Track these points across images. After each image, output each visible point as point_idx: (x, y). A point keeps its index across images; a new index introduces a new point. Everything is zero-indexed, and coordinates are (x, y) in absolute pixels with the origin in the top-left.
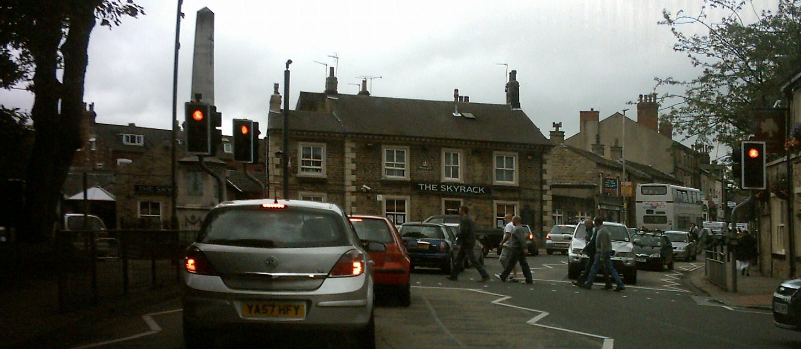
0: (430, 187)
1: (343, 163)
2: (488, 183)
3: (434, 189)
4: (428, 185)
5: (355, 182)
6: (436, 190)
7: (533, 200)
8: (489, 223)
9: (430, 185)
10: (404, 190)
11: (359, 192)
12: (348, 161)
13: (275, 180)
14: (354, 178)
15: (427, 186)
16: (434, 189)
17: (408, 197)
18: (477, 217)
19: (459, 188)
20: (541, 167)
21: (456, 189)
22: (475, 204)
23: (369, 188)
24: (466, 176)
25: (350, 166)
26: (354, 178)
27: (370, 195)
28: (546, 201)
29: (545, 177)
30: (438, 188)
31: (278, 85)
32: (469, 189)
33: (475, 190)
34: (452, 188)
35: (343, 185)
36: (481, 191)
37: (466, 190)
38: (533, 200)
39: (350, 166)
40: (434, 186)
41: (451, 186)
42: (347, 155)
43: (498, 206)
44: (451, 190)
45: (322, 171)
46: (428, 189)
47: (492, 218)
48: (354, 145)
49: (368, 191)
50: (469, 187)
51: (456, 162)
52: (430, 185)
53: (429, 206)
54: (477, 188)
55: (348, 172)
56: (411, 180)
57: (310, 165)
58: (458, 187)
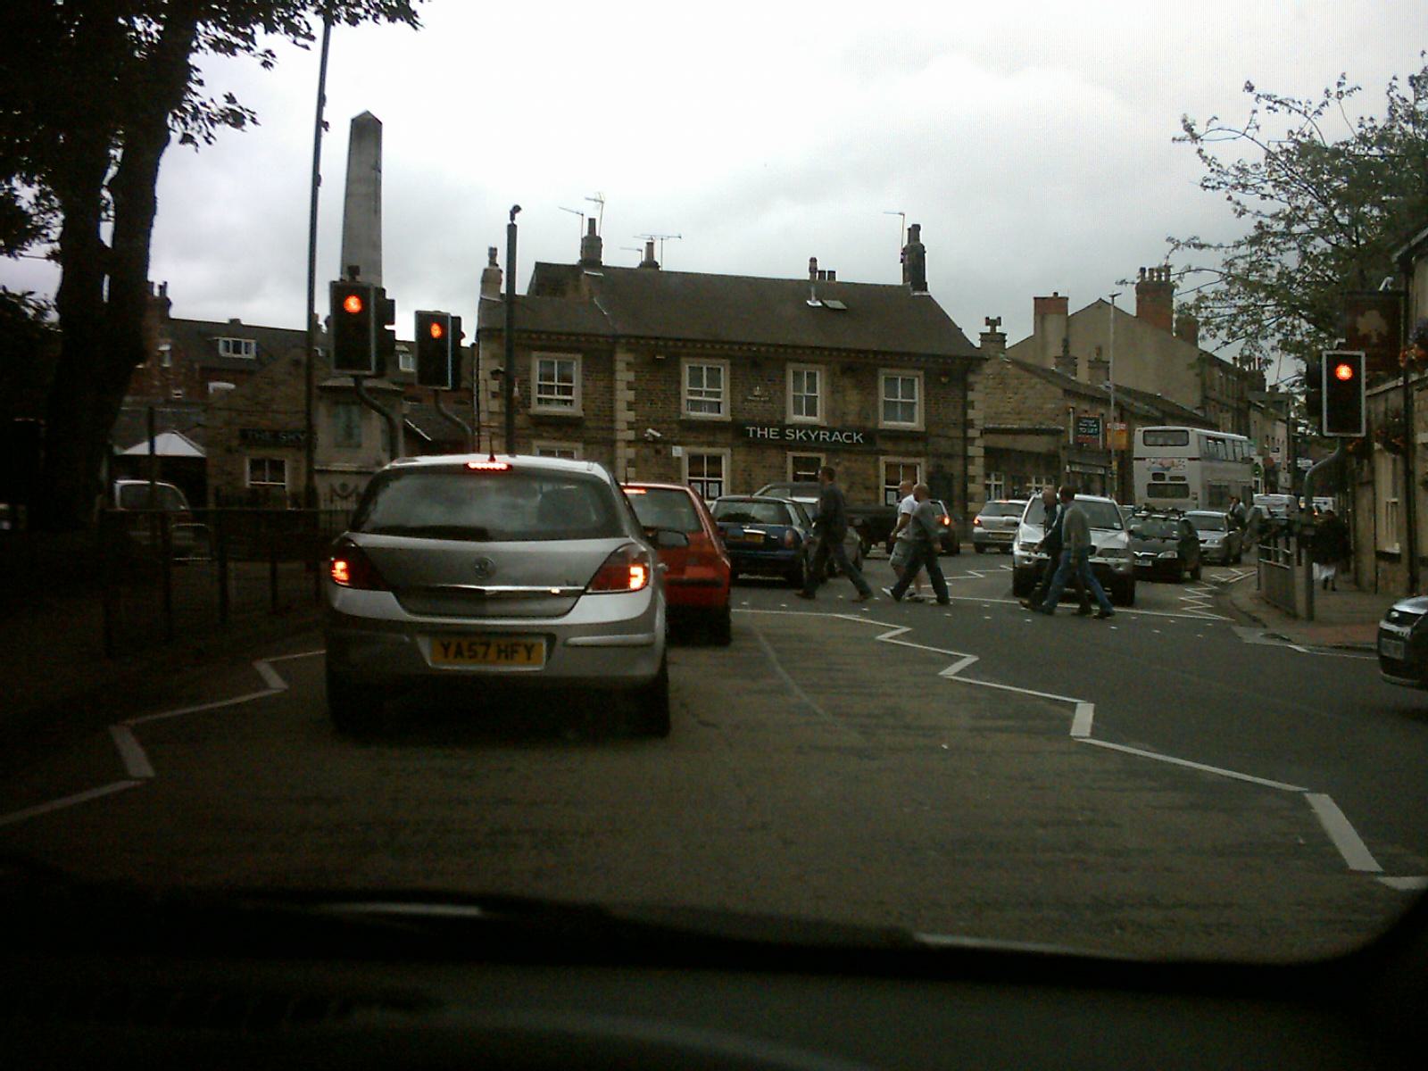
0: (766, 433)
1: (611, 389)
2: (870, 425)
4: (762, 429)
5: (633, 423)
6: (777, 437)
7: (950, 456)
8: (872, 497)
10: (720, 437)
11: (641, 441)
12: (620, 385)
13: (490, 420)
14: (631, 416)
15: (761, 430)
17: (728, 451)
19: (818, 434)
20: (965, 396)
21: (813, 437)
22: (847, 464)
23: (659, 435)
24: (831, 413)
25: (624, 396)
26: (631, 416)
27: (659, 446)
28: (973, 457)
29: (971, 414)
30: (782, 434)
31: (496, 249)
32: (837, 436)
33: (847, 437)
35: (612, 430)
36: (857, 440)
37: (830, 438)
38: (950, 456)
39: (624, 396)
41: (804, 432)
42: (619, 376)
43: (889, 466)
44: (805, 438)
45: (575, 404)
46: (762, 435)
47: (878, 488)
48: (630, 358)
49: (656, 441)
50: (837, 433)
51: (812, 388)
53: (764, 467)
55: (621, 405)
56: (733, 419)
57: (553, 393)
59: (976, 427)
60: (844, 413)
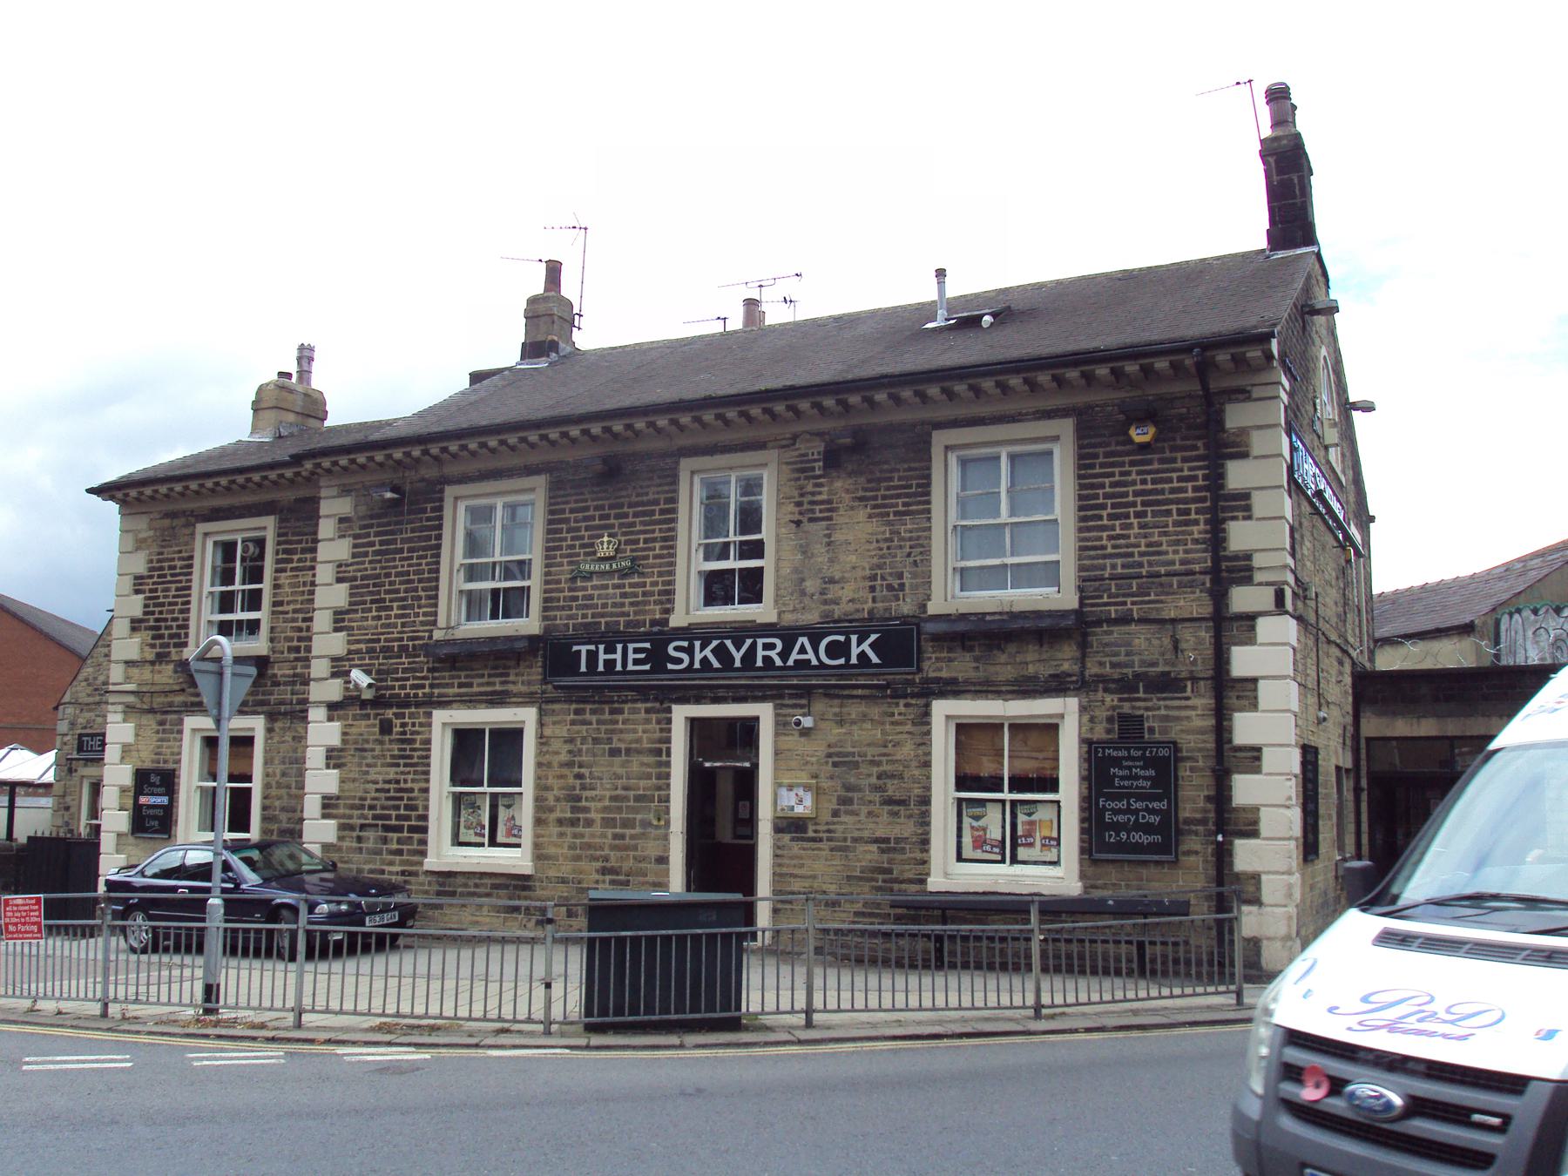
2: (906, 607)
3: (636, 662)
4: (610, 649)
6: (647, 667)
7: (1167, 684)
9: (619, 647)
13: (128, 679)
16: (636, 662)
18: (844, 801)
19: (753, 646)
20: (1216, 478)
21: (738, 656)
25: (331, 595)
27: (389, 713)
28: (1254, 680)
29: (1240, 535)
30: (657, 657)
32: (803, 650)
33: (835, 650)
34: (721, 652)
36: (862, 655)
38: (1167, 684)
39: (331, 595)
40: (636, 651)
41: (715, 643)
43: (965, 731)
44: (716, 664)
47: (925, 801)
48: (344, 506)
50: (804, 640)
52: (619, 647)
53: (614, 752)
54: (842, 638)
56: (547, 629)
58: (749, 642)
59: (1259, 577)
60: (832, 581)
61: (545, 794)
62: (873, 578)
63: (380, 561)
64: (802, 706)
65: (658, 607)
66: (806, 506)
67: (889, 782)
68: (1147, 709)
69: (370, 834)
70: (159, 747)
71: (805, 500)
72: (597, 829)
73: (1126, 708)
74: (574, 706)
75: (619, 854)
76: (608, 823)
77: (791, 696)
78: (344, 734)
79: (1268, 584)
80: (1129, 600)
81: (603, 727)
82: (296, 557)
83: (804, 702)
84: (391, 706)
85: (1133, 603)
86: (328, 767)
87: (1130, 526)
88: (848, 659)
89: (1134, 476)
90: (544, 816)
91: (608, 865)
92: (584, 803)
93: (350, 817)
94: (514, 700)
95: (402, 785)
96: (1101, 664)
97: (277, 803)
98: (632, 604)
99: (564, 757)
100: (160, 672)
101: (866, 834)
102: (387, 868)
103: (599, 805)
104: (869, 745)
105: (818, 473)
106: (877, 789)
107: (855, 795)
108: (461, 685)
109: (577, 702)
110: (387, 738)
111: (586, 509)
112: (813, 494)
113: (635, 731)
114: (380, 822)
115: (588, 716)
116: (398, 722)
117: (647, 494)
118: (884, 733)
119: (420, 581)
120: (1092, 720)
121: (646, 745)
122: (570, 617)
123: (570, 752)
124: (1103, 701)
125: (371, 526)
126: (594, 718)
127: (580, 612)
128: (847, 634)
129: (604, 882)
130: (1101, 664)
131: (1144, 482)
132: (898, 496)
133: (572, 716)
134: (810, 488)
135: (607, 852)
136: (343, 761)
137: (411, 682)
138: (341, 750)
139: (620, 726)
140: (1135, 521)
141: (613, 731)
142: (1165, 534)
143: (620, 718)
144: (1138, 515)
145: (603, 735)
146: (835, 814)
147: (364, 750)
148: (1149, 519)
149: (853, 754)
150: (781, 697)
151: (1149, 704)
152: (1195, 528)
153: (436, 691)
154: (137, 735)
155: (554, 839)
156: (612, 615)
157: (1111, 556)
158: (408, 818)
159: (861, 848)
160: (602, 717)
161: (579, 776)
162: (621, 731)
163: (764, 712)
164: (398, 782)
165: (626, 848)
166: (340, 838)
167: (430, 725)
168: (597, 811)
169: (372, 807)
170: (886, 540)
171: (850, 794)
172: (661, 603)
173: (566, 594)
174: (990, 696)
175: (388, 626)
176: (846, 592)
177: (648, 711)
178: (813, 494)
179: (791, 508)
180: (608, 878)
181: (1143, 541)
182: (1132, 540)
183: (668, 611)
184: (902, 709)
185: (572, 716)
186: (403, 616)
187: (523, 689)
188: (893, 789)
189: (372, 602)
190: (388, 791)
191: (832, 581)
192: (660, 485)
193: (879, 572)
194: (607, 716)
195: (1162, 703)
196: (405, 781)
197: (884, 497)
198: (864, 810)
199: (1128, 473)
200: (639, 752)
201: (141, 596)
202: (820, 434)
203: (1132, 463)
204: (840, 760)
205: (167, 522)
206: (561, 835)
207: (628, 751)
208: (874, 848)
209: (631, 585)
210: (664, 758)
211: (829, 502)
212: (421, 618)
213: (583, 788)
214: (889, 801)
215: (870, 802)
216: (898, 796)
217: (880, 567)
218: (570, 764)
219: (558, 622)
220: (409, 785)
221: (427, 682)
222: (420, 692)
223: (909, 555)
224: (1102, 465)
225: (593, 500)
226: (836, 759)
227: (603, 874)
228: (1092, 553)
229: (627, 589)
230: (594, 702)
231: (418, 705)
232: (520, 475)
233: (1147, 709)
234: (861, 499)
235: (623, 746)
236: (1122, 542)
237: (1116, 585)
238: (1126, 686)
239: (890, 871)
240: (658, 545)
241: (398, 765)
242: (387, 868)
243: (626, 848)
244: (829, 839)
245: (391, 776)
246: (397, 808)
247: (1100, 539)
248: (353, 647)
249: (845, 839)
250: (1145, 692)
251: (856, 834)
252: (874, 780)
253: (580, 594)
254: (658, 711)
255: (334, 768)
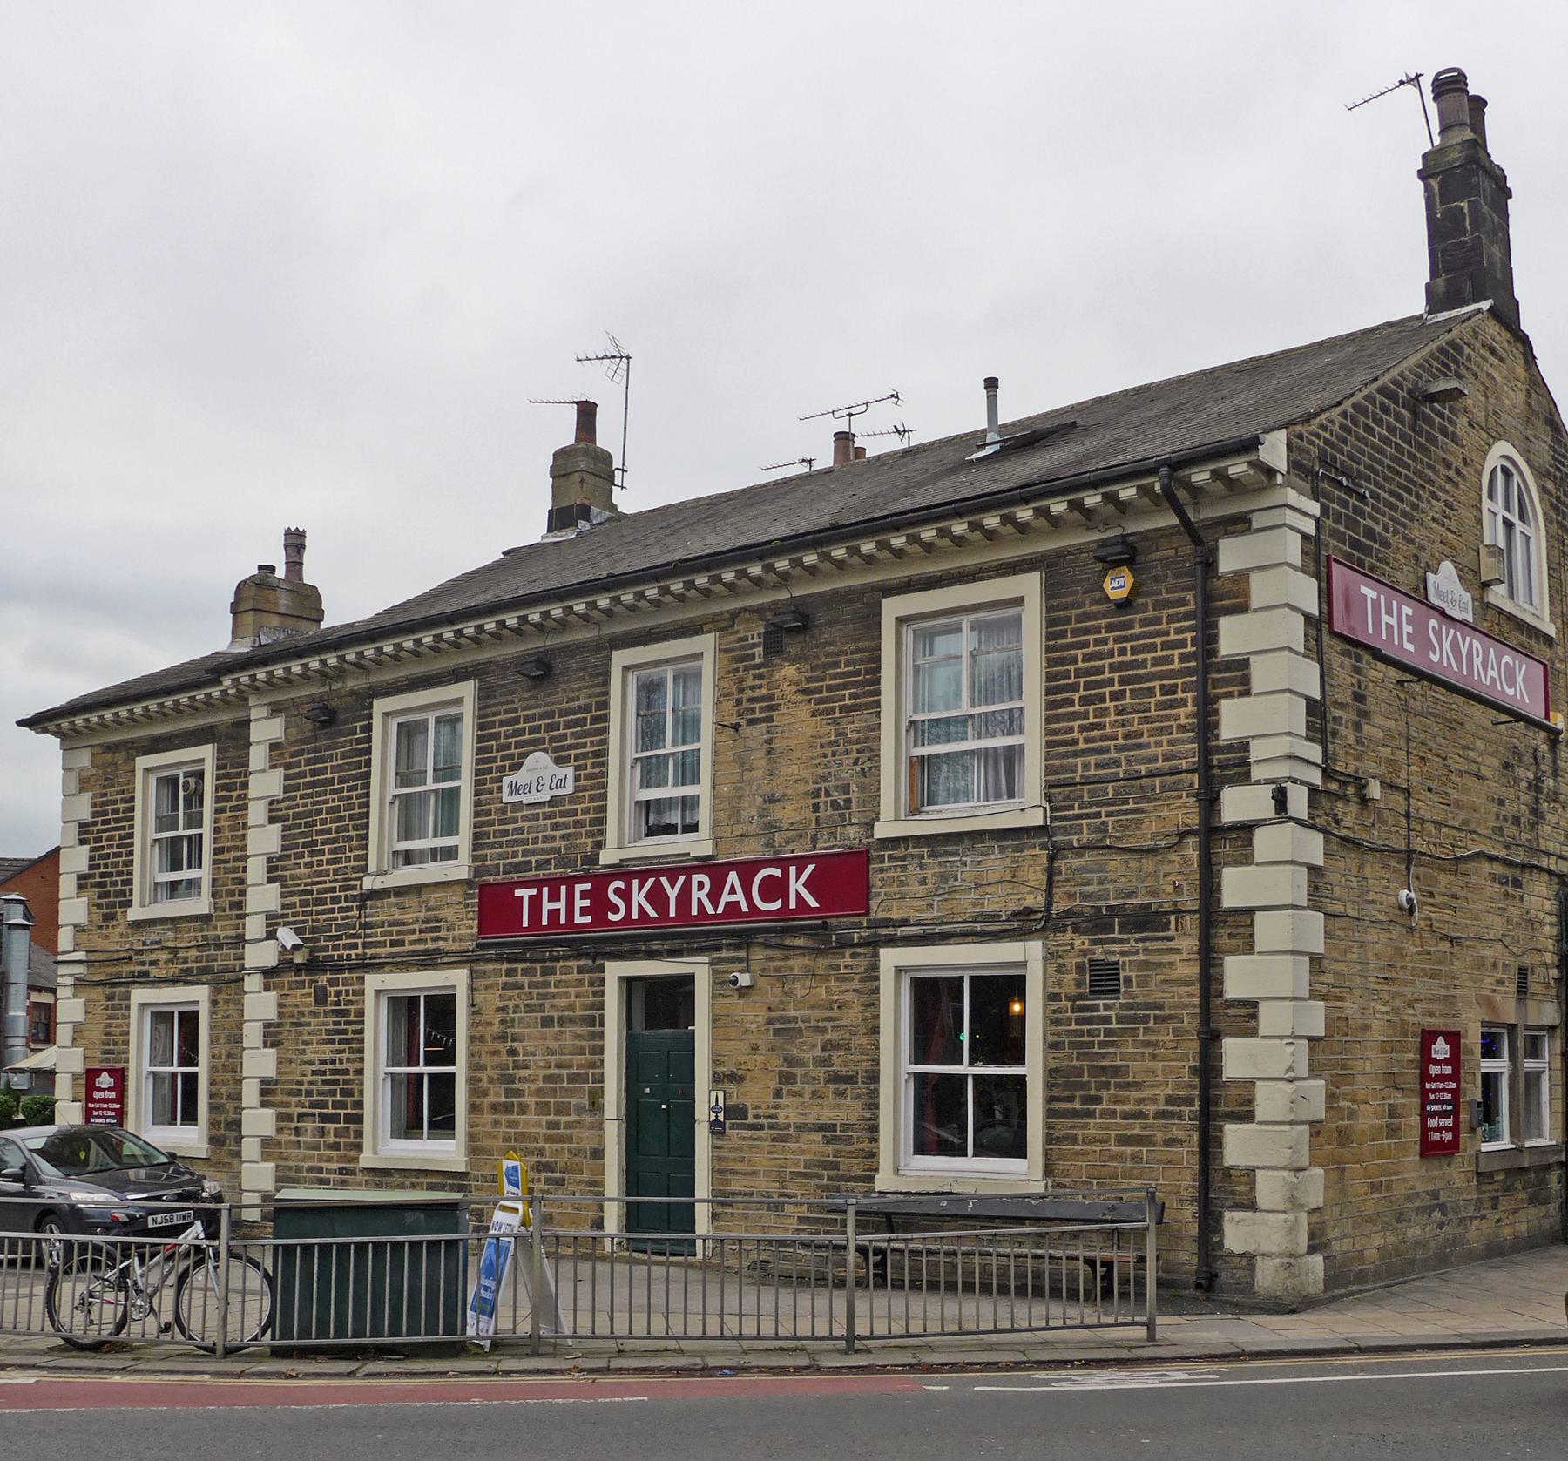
0: (561, 905)
7: (1146, 921)
8: (852, 1112)
18: (787, 1078)
22: (774, 995)
27: (323, 979)
28: (1250, 912)
37: (714, 897)
38: (1146, 921)
46: (554, 914)
53: (547, 1022)
54: (777, 872)
58: (682, 879)
59: (1257, 773)
60: (771, 800)
61: (479, 1074)
62: (817, 794)
63: (310, 795)
64: (740, 960)
65: (589, 840)
66: (745, 705)
67: (835, 1054)
68: (1123, 953)
69: (309, 1125)
70: (109, 1026)
71: (745, 697)
72: (531, 1116)
73: (1099, 953)
74: (506, 966)
75: (555, 1146)
76: (543, 1108)
77: (730, 947)
78: (281, 1005)
79: (1268, 782)
80: (1103, 810)
81: (535, 991)
82: (234, 794)
83: (742, 954)
84: (325, 972)
85: (1109, 815)
86: (265, 1046)
87: (1103, 713)
88: (786, 902)
89: (1111, 645)
90: (478, 1101)
91: (544, 1160)
92: (517, 1085)
93: (288, 1105)
94: (446, 960)
95: (338, 1066)
96: (1071, 896)
97: (223, 1090)
98: (562, 837)
99: (496, 1029)
100: (107, 937)
101: (810, 1120)
102: (325, 1165)
103: (533, 1086)
104: (812, 1007)
105: (758, 661)
106: (824, 1062)
107: (799, 1071)
108: (393, 944)
109: (509, 961)
110: (321, 1010)
111: (516, 720)
112: (752, 688)
113: (567, 995)
114: (317, 1111)
115: (519, 978)
116: (331, 990)
117: (578, 698)
118: (829, 991)
119: (351, 818)
120: (1060, 969)
121: (579, 1013)
122: (501, 856)
123: (502, 1022)
124: (1072, 945)
125: (301, 753)
126: (526, 980)
127: (510, 850)
128: (783, 864)
129: (539, 1180)
130: (1071, 896)
131: (1122, 652)
132: (844, 686)
133: (504, 979)
134: (749, 682)
135: (541, 1144)
136: (280, 1038)
137: (344, 942)
138: (279, 1025)
139: (552, 990)
140: (1109, 704)
141: (545, 996)
142: (1146, 720)
143: (552, 978)
144: (1116, 697)
145: (534, 1001)
146: (778, 1094)
147: (301, 1025)
148: (1128, 701)
149: (795, 1019)
150: (718, 948)
151: (1126, 947)
152: (1182, 711)
153: (369, 951)
154: (87, 1013)
155: (489, 1128)
156: (543, 852)
157: (1084, 752)
158: (343, 1105)
159: (806, 1136)
160: (535, 979)
161: (513, 1052)
162: (554, 996)
163: (699, 969)
164: (333, 1062)
165: (561, 1139)
166: (280, 1130)
167: (363, 993)
168: (530, 1095)
169: (309, 1093)
170: (831, 743)
171: (793, 1070)
172: (593, 835)
173: (496, 827)
174: (970, 939)
175: (320, 874)
176: (787, 814)
177: (580, 970)
178: (752, 688)
179: (729, 706)
180: (543, 1175)
181: (1121, 731)
182: (1108, 730)
183: (600, 845)
184: (848, 960)
185: (504, 979)
186: (335, 861)
187: (455, 946)
188: (838, 1061)
189: (305, 845)
190: (323, 1073)
191: (771, 800)
192: (592, 687)
193: (823, 785)
194: (539, 978)
195: (1140, 945)
196: (341, 1061)
197: (830, 688)
198: (809, 1088)
199: (1105, 641)
200: (572, 1021)
201: (87, 847)
202: (759, 611)
203: (1110, 628)
204: (784, 1029)
205: (109, 757)
206: (496, 1123)
207: (561, 1023)
208: (818, 1136)
209: (563, 814)
210: (598, 1028)
211: (771, 697)
212: (352, 864)
213: (517, 1066)
214: (835, 1078)
215: (814, 1079)
216: (846, 1070)
217: (824, 779)
218: (502, 1038)
219: (488, 863)
220: (344, 1066)
221: (359, 941)
222: (353, 952)
223: (856, 762)
224: (1075, 633)
225: (524, 709)
226: (778, 1026)
227: (539, 1171)
228: (1061, 750)
229: (558, 819)
230: (525, 961)
231: (351, 968)
232: (449, 682)
233: (1123, 953)
234: (804, 692)
235: (555, 1014)
236: (1096, 733)
237: (1089, 791)
238: (1097, 923)
239: (835, 1166)
240: (589, 762)
241: (332, 1042)
242: (325, 1165)
243: (561, 1139)
244: (771, 1127)
245: (328, 1056)
246: (333, 1093)
247: (1071, 730)
248: (287, 901)
249: (788, 1126)
250: (1121, 932)
251: (800, 1120)
252: (818, 1052)
253: (510, 827)
254: (591, 971)
255: (272, 1047)
